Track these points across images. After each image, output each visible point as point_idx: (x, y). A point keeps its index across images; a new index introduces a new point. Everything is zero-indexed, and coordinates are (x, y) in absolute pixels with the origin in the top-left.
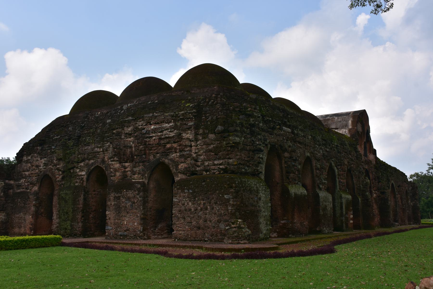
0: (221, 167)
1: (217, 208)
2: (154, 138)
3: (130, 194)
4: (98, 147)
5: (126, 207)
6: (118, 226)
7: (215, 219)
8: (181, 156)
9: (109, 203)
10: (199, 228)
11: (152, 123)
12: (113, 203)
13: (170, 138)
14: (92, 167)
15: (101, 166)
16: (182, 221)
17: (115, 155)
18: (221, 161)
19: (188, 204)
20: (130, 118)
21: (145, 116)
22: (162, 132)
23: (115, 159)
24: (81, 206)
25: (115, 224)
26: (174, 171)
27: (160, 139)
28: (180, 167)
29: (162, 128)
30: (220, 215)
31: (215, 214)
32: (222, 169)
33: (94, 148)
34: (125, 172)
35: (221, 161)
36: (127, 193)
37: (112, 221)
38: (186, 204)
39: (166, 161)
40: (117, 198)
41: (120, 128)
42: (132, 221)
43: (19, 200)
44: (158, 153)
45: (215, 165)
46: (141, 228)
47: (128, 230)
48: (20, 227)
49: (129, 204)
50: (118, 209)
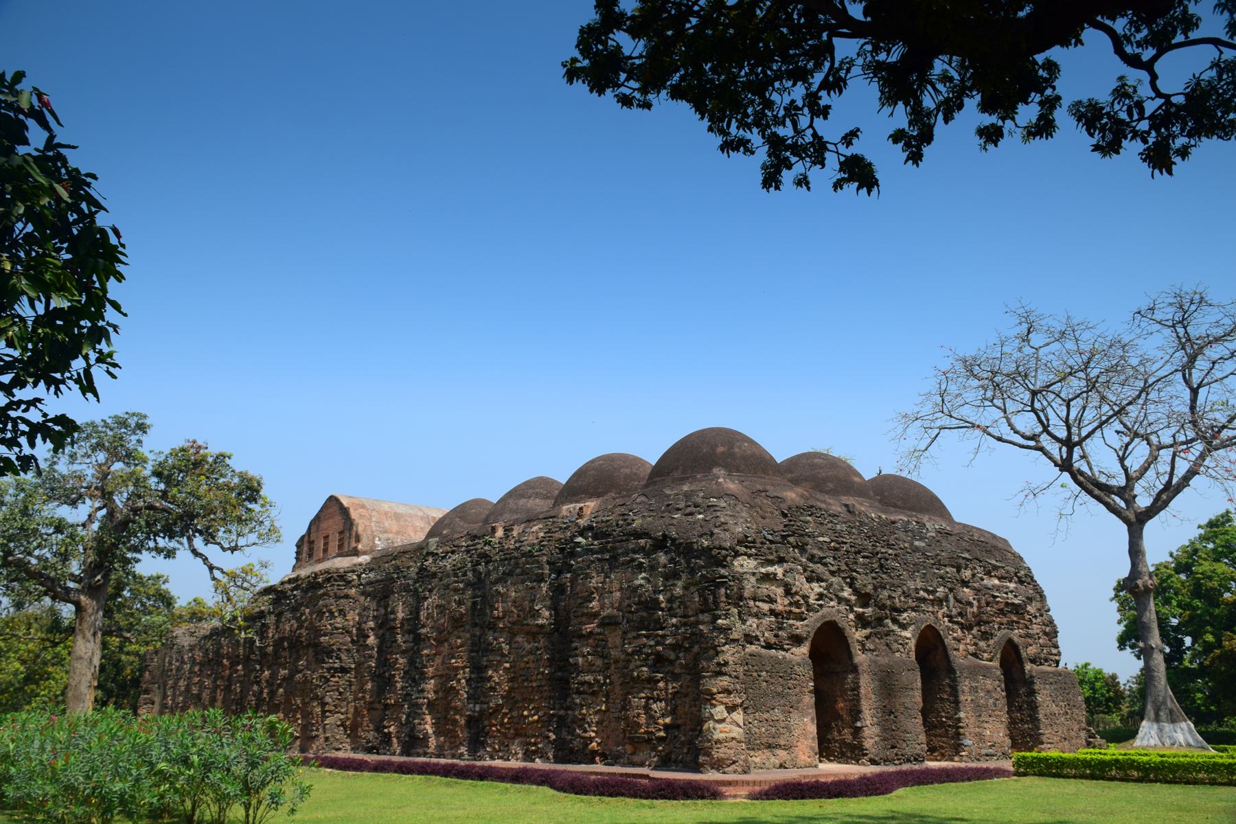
4: (926, 590)
6: (980, 737)
7: (1076, 727)
9: (962, 698)
20: (966, 555)
24: (919, 699)
40: (974, 690)
42: (996, 730)
46: (1008, 741)
49: (991, 701)
50: (978, 709)
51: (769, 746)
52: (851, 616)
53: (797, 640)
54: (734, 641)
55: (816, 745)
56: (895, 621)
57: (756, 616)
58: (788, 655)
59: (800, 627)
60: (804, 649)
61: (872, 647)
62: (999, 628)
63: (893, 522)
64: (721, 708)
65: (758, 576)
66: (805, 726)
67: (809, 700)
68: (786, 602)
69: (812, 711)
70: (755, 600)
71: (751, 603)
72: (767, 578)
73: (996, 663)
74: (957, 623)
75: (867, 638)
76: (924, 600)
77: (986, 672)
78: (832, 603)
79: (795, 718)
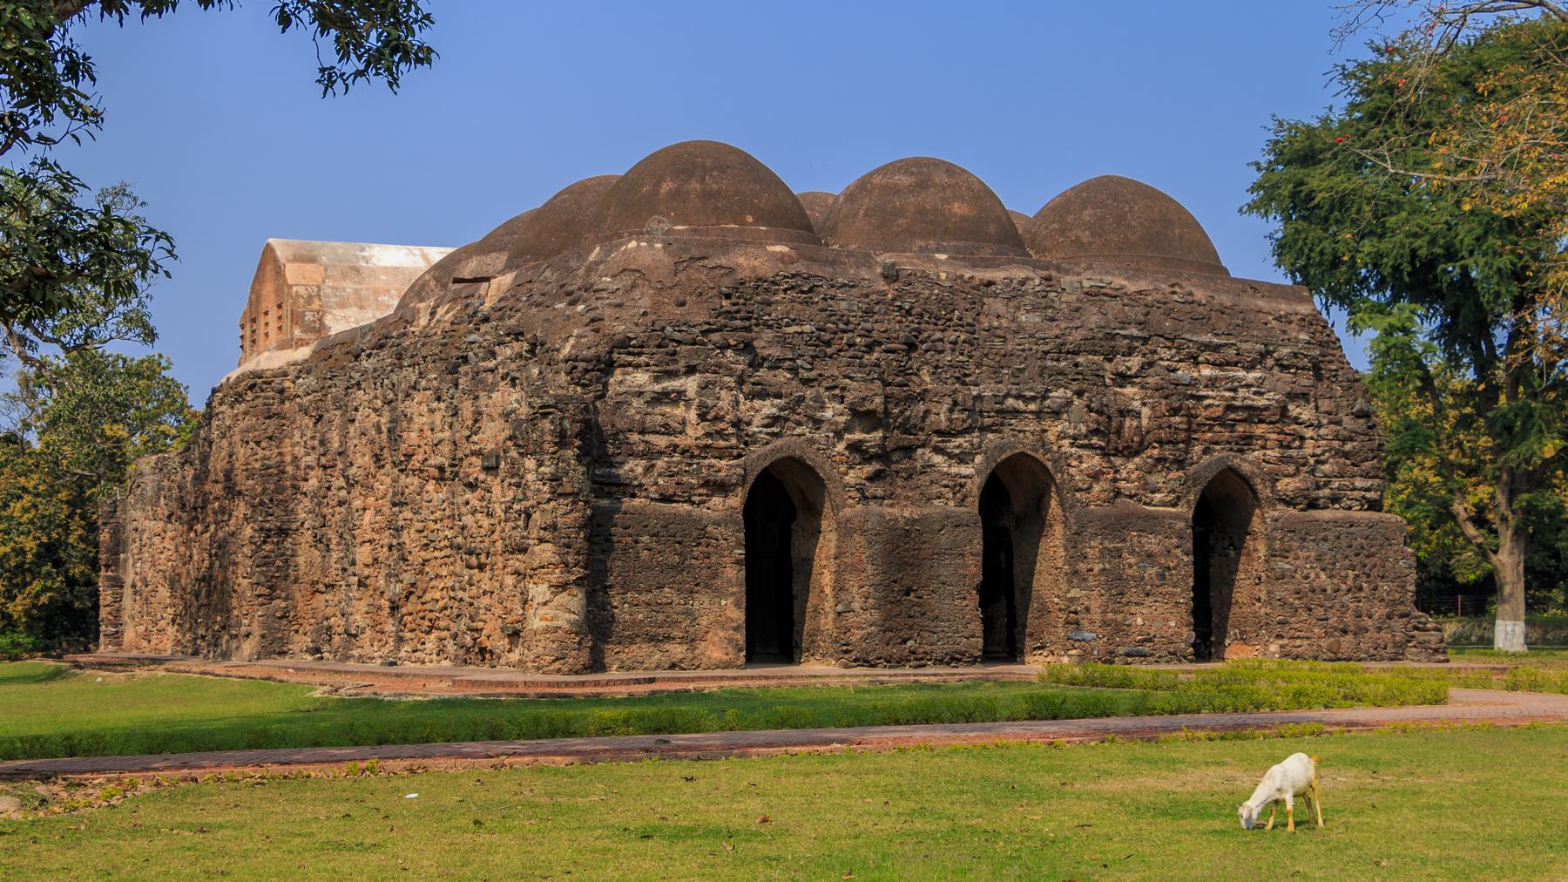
0: (1368, 495)
1: (1385, 587)
2: (1207, 402)
3: (1152, 543)
4: (1018, 397)
5: (1143, 578)
6: (1118, 628)
7: (1385, 611)
8: (1283, 460)
10: (1345, 632)
11: (1201, 359)
12: (1097, 568)
13: (1258, 408)
14: (1004, 457)
15: (1039, 456)
16: (1305, 616)
17: (1096, 432)
18: (1369, 483)
19: (1317, 576)
21: (1187, 336)
22: (1235, 390)
23: (1095, 440)
25: (1105, 624)
26: (1265, 492)
27: (1230, 408)
28: (1279, 485)
29: (1239, 380)
30: (1394, 603)
31: (1382, 600)
32: (1369, 501)
33: (1007, 395)
34: (1115, 480)
35: (1369, 483)
36: (1144, 540)
37: (1097, 617)
38: (1313, 576)
39: (1246, 468)
41: (1095, 353)
43: (645, 538)
44: (1217, 443)
45: (1354, 489)
47: (1150, 640)
48: (691, 641)
49: (1153, 571)
51: (652, 639)
52: (841, 447)
53: (722, 488)
54: (560, 495)
55: (741, 637)
56: (938, 450)
57: (642, 455)
58: (696, 511)
59: (724, 468)
60: (736, 501)
61: (880, 492)
62: (1206, 451)
63: (990, 284)
64: (546, 585)
65: (648, 397)
66: (723, 612)
67: (733, 574)
68: (700, 433)
69: (739, 590)
70: (642, 432)
71: (635, 437)
72: (661, 398)
73: (1185, 510)
74: (1090, 447)
75: (870, 479)
76: (1016, 412)
77: (1151, 523)
78: (799, 430)
79: (702, 601)
